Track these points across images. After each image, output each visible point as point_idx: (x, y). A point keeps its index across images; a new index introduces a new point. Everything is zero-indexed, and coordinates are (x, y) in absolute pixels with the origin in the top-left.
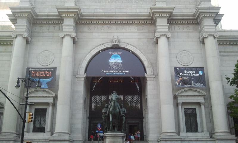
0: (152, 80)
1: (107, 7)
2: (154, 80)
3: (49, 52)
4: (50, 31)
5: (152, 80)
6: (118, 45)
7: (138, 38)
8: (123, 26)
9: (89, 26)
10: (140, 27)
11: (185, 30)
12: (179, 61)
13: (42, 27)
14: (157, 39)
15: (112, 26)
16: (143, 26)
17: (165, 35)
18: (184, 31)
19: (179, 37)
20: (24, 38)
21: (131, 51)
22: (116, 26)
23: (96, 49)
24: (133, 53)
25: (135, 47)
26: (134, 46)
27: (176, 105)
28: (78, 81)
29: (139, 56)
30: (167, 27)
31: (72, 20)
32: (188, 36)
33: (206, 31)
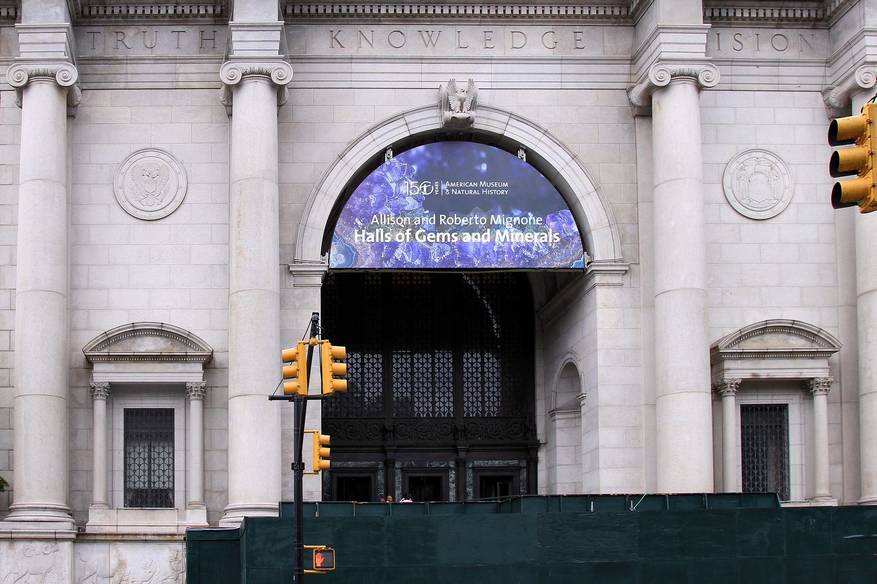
0: (614, 285)
2: (622, 285)
3: (162, 156)
4: (158, 52)
5: (614, 285)
6: (472, 122)
7: (558, 86)
8: (491, 28)
9: (332, 28)
10: (566, 34)
11: (766, 52)
12: (731, 198)
13: (120, 37)
14: (650, 92)
15: (439, 28)
16: (578, 29)
17: (694, 77)
18: (760, 55)
19: (734, 87)
20: (60, 88)
21: (527, 151)
22: (459, 28)
23: (369, 139)
24: (533, 159)
25: (545, 132)
26: (537, 127)
27: (718, 392)
28: (298, 291)
29: (562, 173)
32: (775, 80)
33: (869, 59)
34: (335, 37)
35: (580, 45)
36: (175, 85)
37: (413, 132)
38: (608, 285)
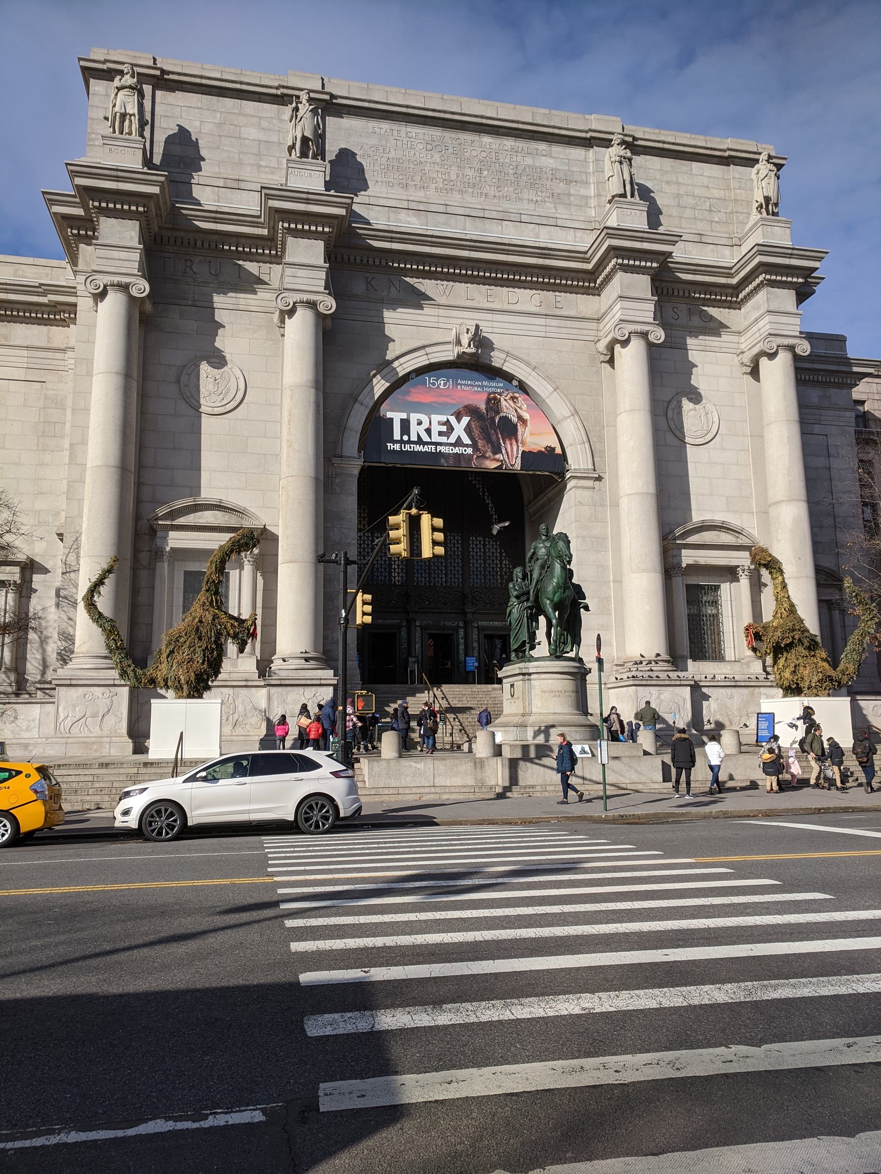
1: (433, 208)
5: (588, 488)
7: (543, 334)
12: (673, 427)
30: (651, 307)
31: (320, 245)
35: (558, 305)
36: (235, 307)
37: (432, 361)
38: (583, 488)
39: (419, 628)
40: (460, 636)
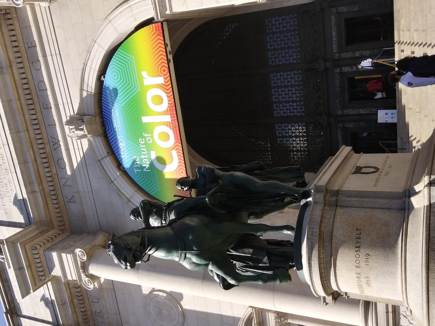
7: (58, 56)
25: (85, 65)
34: (70, 200)
39: (345, 112)
40: (350, 70)
